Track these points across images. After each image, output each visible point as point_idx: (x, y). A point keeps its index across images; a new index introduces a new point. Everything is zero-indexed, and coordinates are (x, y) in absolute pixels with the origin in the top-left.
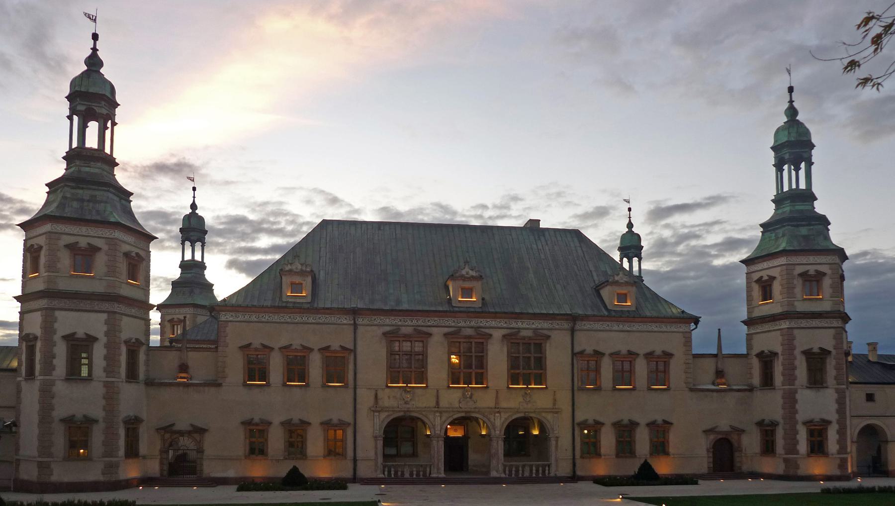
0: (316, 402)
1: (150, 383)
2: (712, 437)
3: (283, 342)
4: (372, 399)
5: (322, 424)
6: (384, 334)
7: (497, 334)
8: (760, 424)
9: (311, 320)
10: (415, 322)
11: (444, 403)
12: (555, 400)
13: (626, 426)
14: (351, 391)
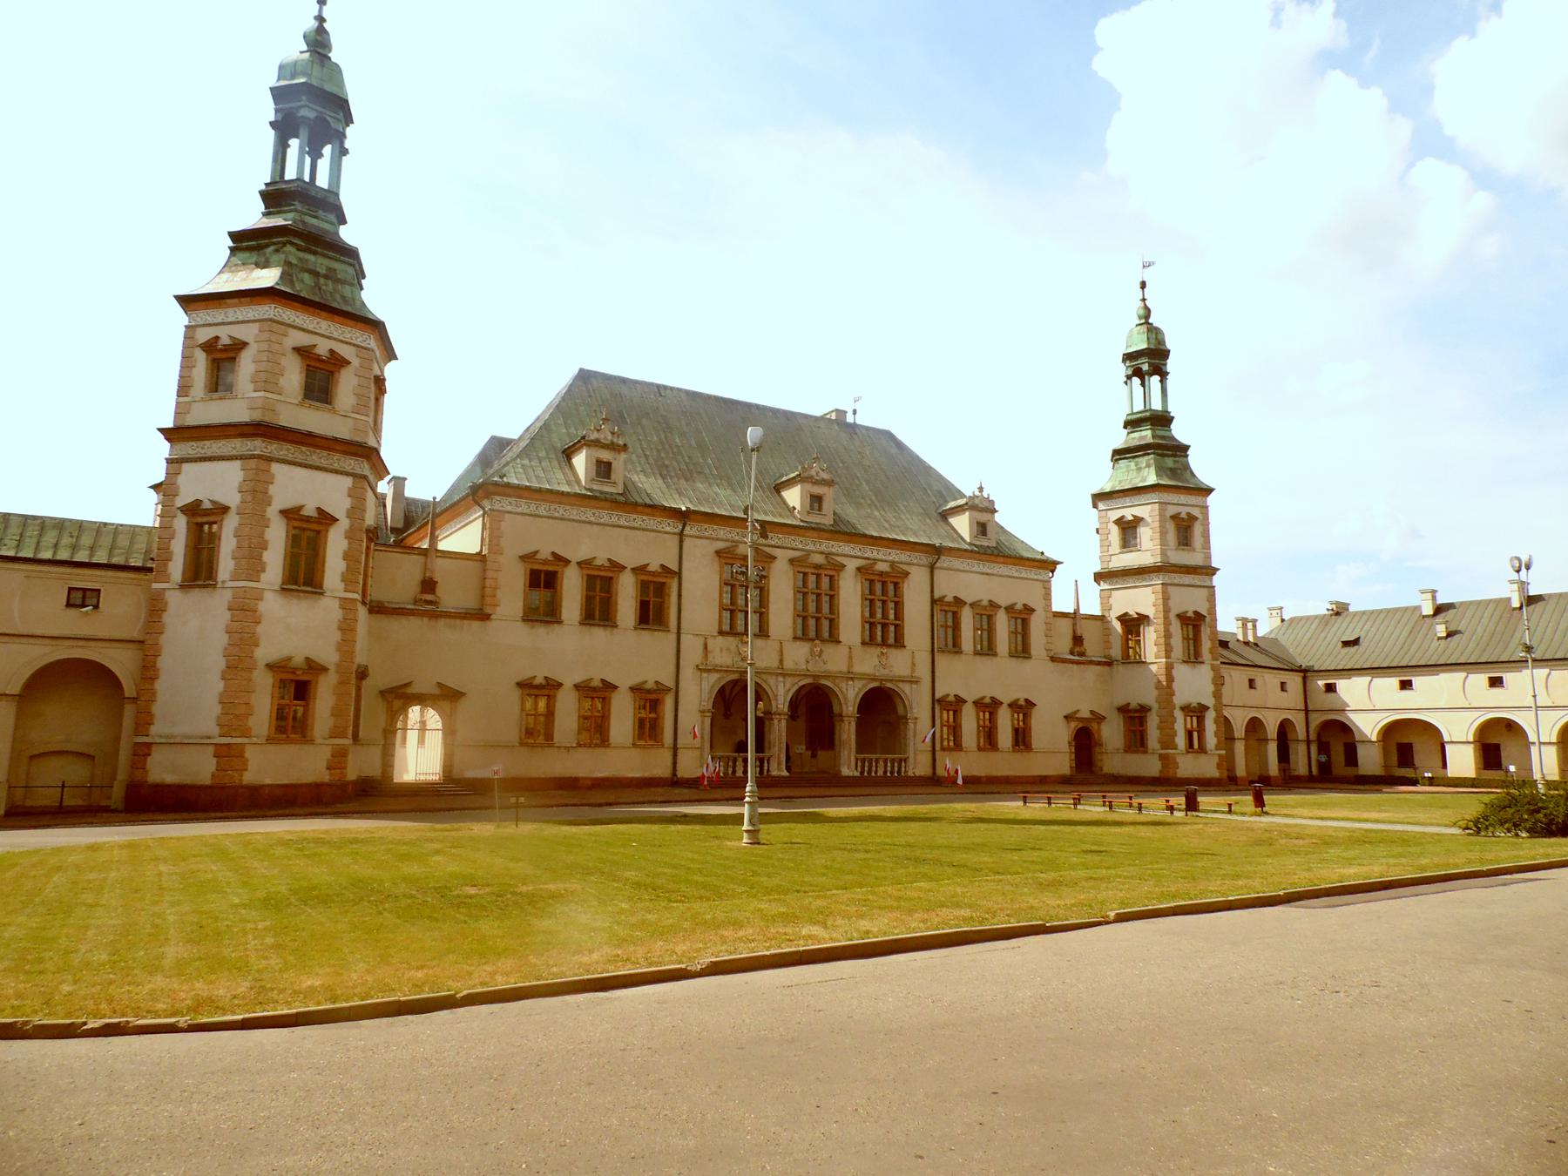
0: (627, 655)
1: (377, 609)
2: (1073, 725)
3: (583, 553)
4: (701, 648)
5: (631, 689)
6: (718, 553)
7: (851, 565)
8: (1124, 710)
9: (622, 522)
12: (914, 665)
13: (987, 706)
14: (672, 637)
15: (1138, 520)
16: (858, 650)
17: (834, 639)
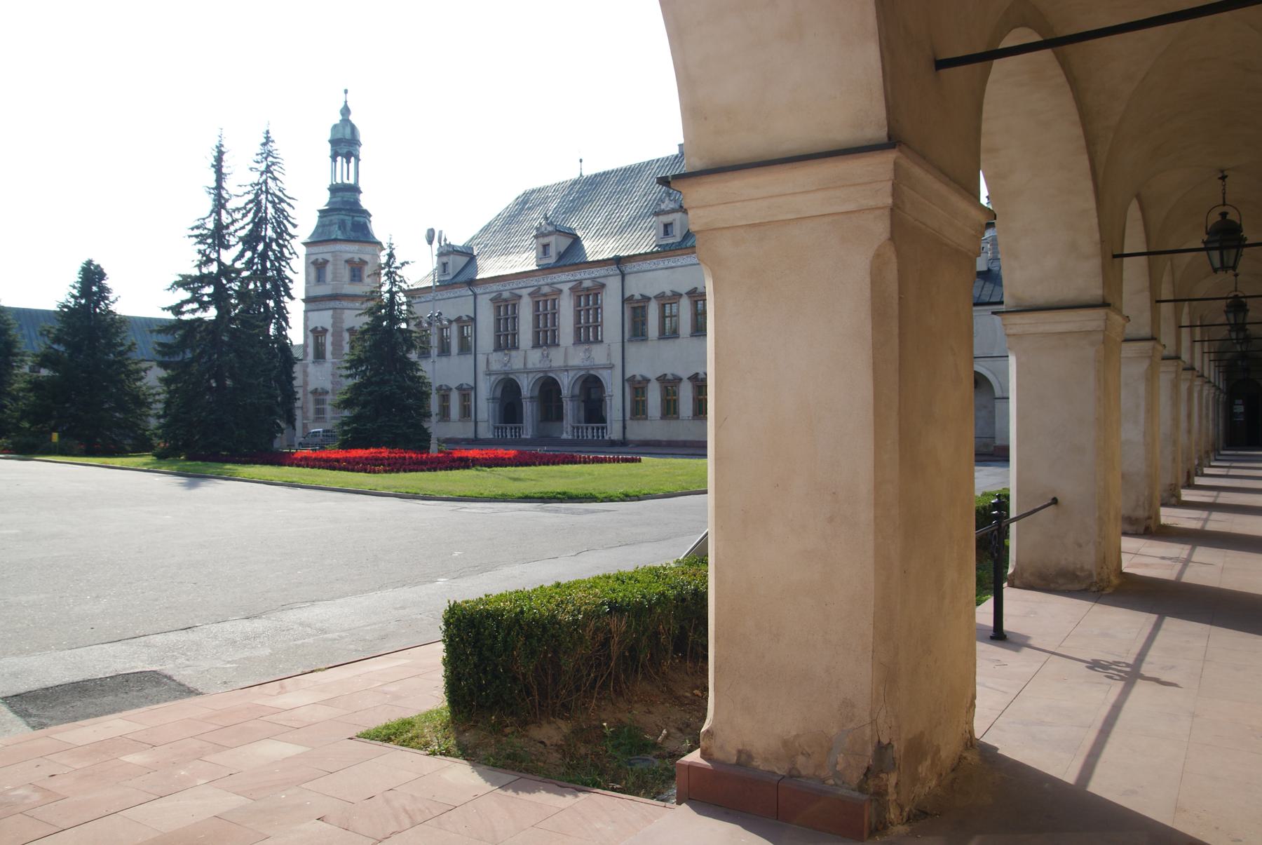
7: (566, 288)
10: (511, 286)
11: (530, 366)
16: (571, 350)
17: (555, 344)
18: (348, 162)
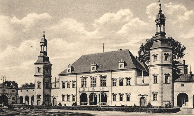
0: (72, 91)
7: (98, 76)
15: (168, 55)
18: (44, 47)
